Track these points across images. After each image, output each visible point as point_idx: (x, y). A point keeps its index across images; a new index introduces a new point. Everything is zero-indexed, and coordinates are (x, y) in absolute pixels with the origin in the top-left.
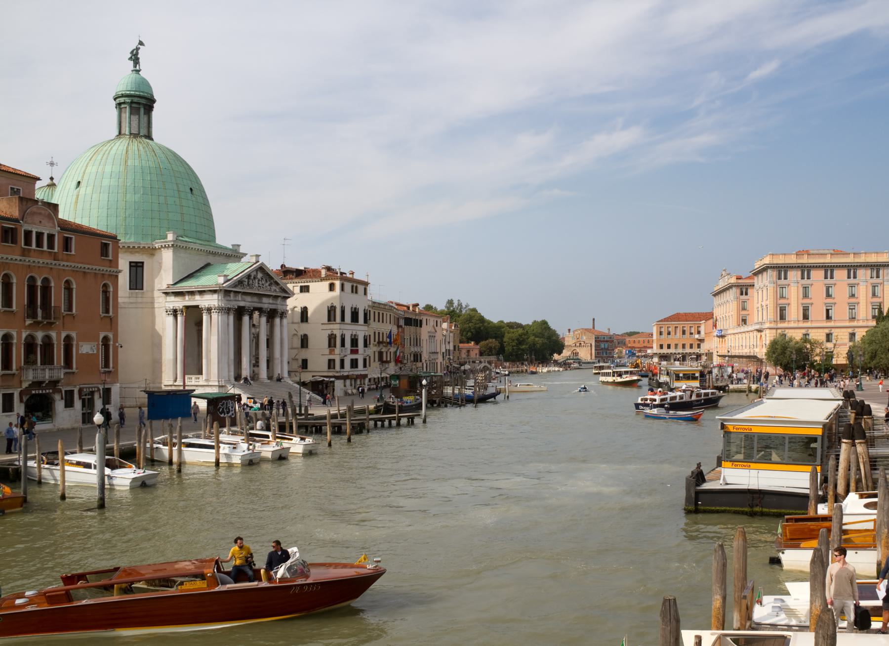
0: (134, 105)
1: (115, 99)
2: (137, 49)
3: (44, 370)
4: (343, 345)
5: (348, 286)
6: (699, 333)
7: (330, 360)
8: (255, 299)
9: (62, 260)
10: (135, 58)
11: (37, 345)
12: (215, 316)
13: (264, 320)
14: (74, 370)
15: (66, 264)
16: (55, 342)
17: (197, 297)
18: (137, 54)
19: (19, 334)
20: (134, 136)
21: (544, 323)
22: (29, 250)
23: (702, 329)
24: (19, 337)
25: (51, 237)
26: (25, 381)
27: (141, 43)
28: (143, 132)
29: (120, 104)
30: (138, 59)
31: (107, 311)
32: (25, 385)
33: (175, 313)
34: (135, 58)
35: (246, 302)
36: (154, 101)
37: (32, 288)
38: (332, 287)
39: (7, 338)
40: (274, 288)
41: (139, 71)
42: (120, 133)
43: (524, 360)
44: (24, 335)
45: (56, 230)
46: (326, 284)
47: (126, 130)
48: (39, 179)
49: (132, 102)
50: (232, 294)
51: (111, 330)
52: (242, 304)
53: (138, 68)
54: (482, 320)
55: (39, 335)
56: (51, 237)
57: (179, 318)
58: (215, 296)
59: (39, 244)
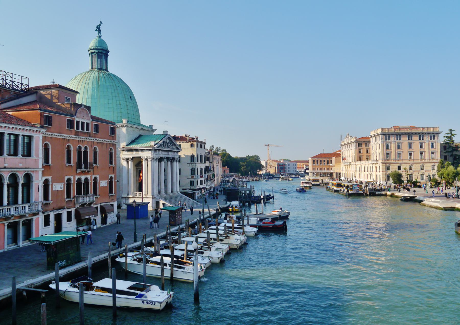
0: (99, 54)
1: (89, 51)
2: (100, 25)
3: (86, 197)
4: (198, 174)
5: (199, 144)
6: (331, 163)
7: (191, 181)
8: (166, 153)
9: (93, 137)
10: (98, 30)
11: (82, 183)
12: (150, 162)
13: (169, 163)
14: (98, 196)
15: (95, 139)
16: (90, 182)
17: (140, 152)
18: (100, 28)
19: (74, 178)
20: (100, 69)
21: (258, 157)
22: (78, 132)
23: (333, 161)
24: (74, 179)
25: (88, 124)
26: (77, 204)
27: (101, 23)
28: (104, 68)
29: (92, 53)
30: (100, 30)
31: (111, 163)
32: (77, 206)
33: (127, 160)
34: (98, 30)
35: (163, 154)
36: (108, 52)
37: (80, 152)
38: (192, 146)
39: (69, 180)
40: (173, 147)
41: (101, 36)
42: (92, 68)
43: (249, 175)
44: (76, 178)
45: (90, 121)
46: (189, 144)
47: (95, 66)
48: (78, 93)
49: (98, 52)
50: (157, 151)
51: (113, 173)
52: (161, 156)
53: (100, 35)
54: (229, 156)
55: (83, 178)
56: (88, 124)
57: (130, 162)
58: (150, 152)
59: (83, 129)
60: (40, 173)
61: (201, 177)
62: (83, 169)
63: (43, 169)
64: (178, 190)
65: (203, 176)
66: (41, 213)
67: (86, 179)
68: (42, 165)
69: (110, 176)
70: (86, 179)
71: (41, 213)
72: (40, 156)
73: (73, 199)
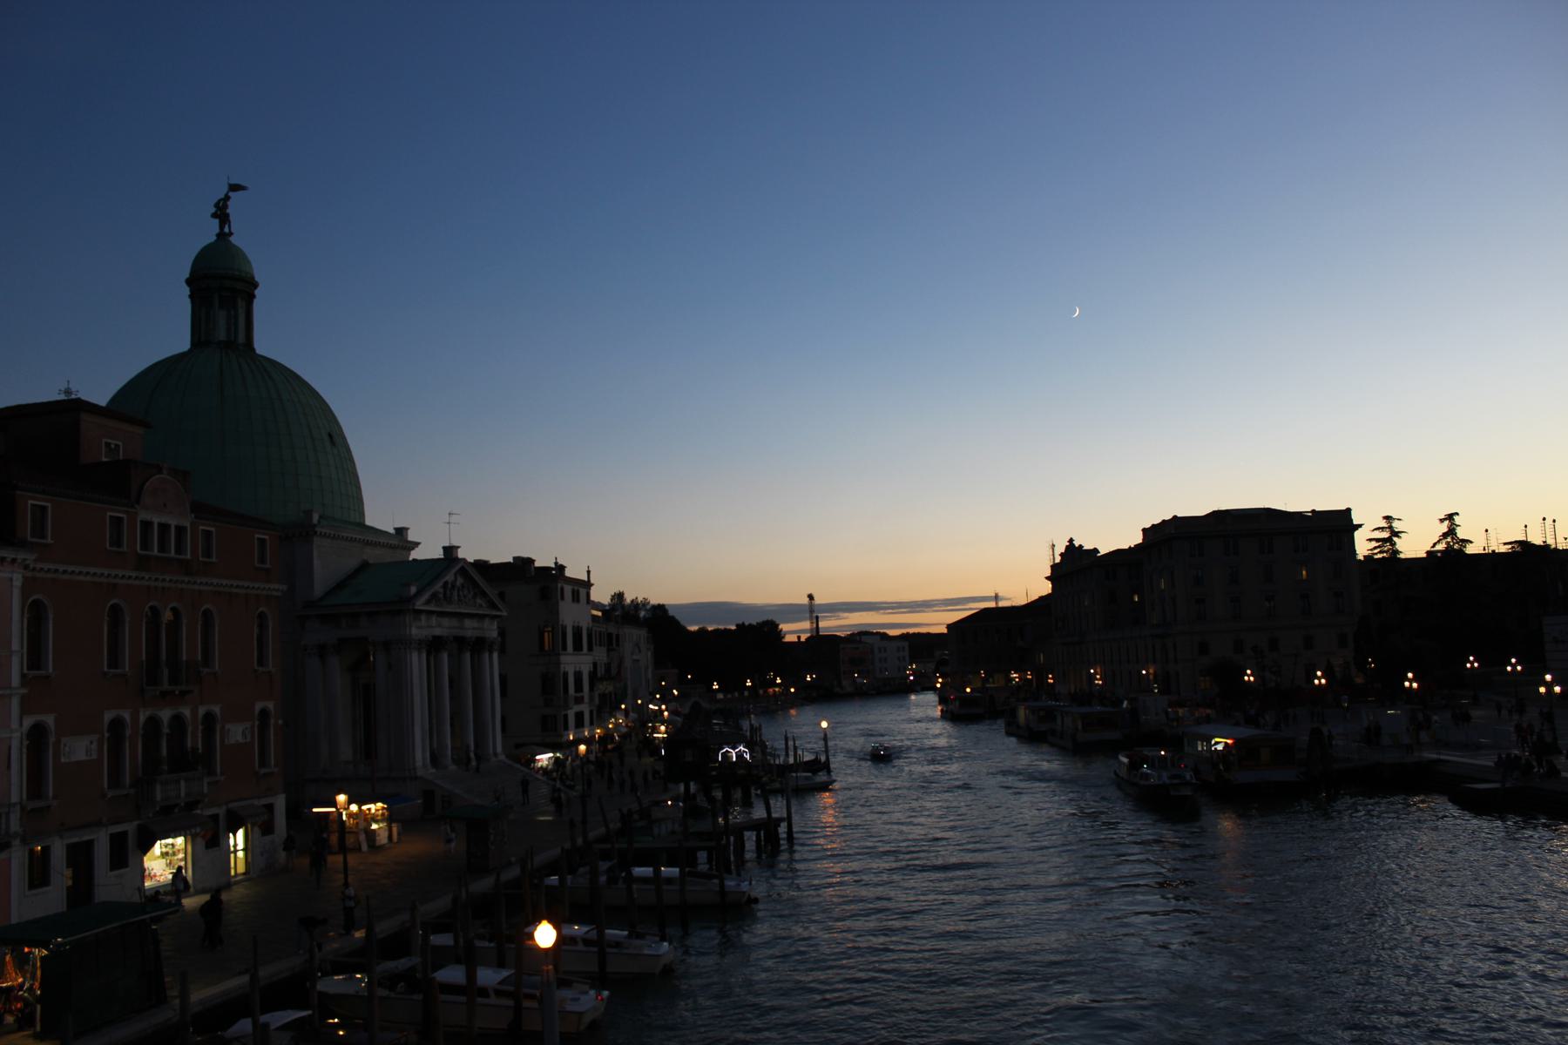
5: (568, 589)
8: (455, 622)
13: (468, 656)
15: (204, 580)
18: (226, 206)
36: (256, 285)
39: (117, 724)
40: (479, 601)
44: (142, 718)
50: (423, 617)
52: (438, 632)
53: (226, 230)
55: (165, 715)
56: (180, 530)
59: (163, 547)
60: (15, 702)
61: (579, 700)
62: (166, 686)
63: (24, 691)
64: (499, 749)
65: (586, 699)
66: (17, 842)
67: (178, 720)
68: (23, 676)
69: (259, 706)
70: (178, 720)
71: (17, 842)
72: (15, 646)
73: (132, 791)
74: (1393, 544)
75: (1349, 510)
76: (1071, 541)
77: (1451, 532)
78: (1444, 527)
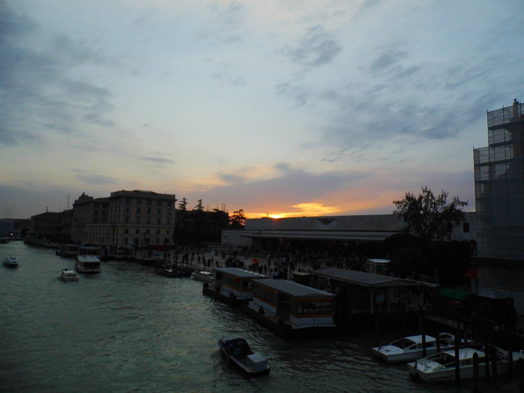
74: (185, 206)
75: (174, 195)
76: (84, 193)
77: (200, 205)
78: (198, 203)
